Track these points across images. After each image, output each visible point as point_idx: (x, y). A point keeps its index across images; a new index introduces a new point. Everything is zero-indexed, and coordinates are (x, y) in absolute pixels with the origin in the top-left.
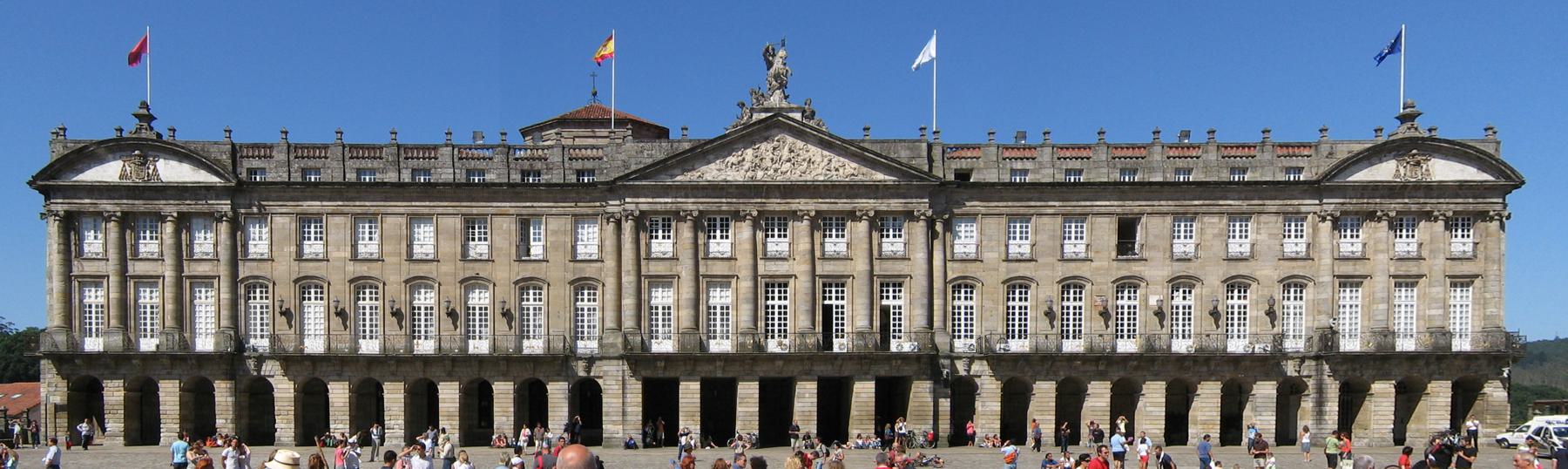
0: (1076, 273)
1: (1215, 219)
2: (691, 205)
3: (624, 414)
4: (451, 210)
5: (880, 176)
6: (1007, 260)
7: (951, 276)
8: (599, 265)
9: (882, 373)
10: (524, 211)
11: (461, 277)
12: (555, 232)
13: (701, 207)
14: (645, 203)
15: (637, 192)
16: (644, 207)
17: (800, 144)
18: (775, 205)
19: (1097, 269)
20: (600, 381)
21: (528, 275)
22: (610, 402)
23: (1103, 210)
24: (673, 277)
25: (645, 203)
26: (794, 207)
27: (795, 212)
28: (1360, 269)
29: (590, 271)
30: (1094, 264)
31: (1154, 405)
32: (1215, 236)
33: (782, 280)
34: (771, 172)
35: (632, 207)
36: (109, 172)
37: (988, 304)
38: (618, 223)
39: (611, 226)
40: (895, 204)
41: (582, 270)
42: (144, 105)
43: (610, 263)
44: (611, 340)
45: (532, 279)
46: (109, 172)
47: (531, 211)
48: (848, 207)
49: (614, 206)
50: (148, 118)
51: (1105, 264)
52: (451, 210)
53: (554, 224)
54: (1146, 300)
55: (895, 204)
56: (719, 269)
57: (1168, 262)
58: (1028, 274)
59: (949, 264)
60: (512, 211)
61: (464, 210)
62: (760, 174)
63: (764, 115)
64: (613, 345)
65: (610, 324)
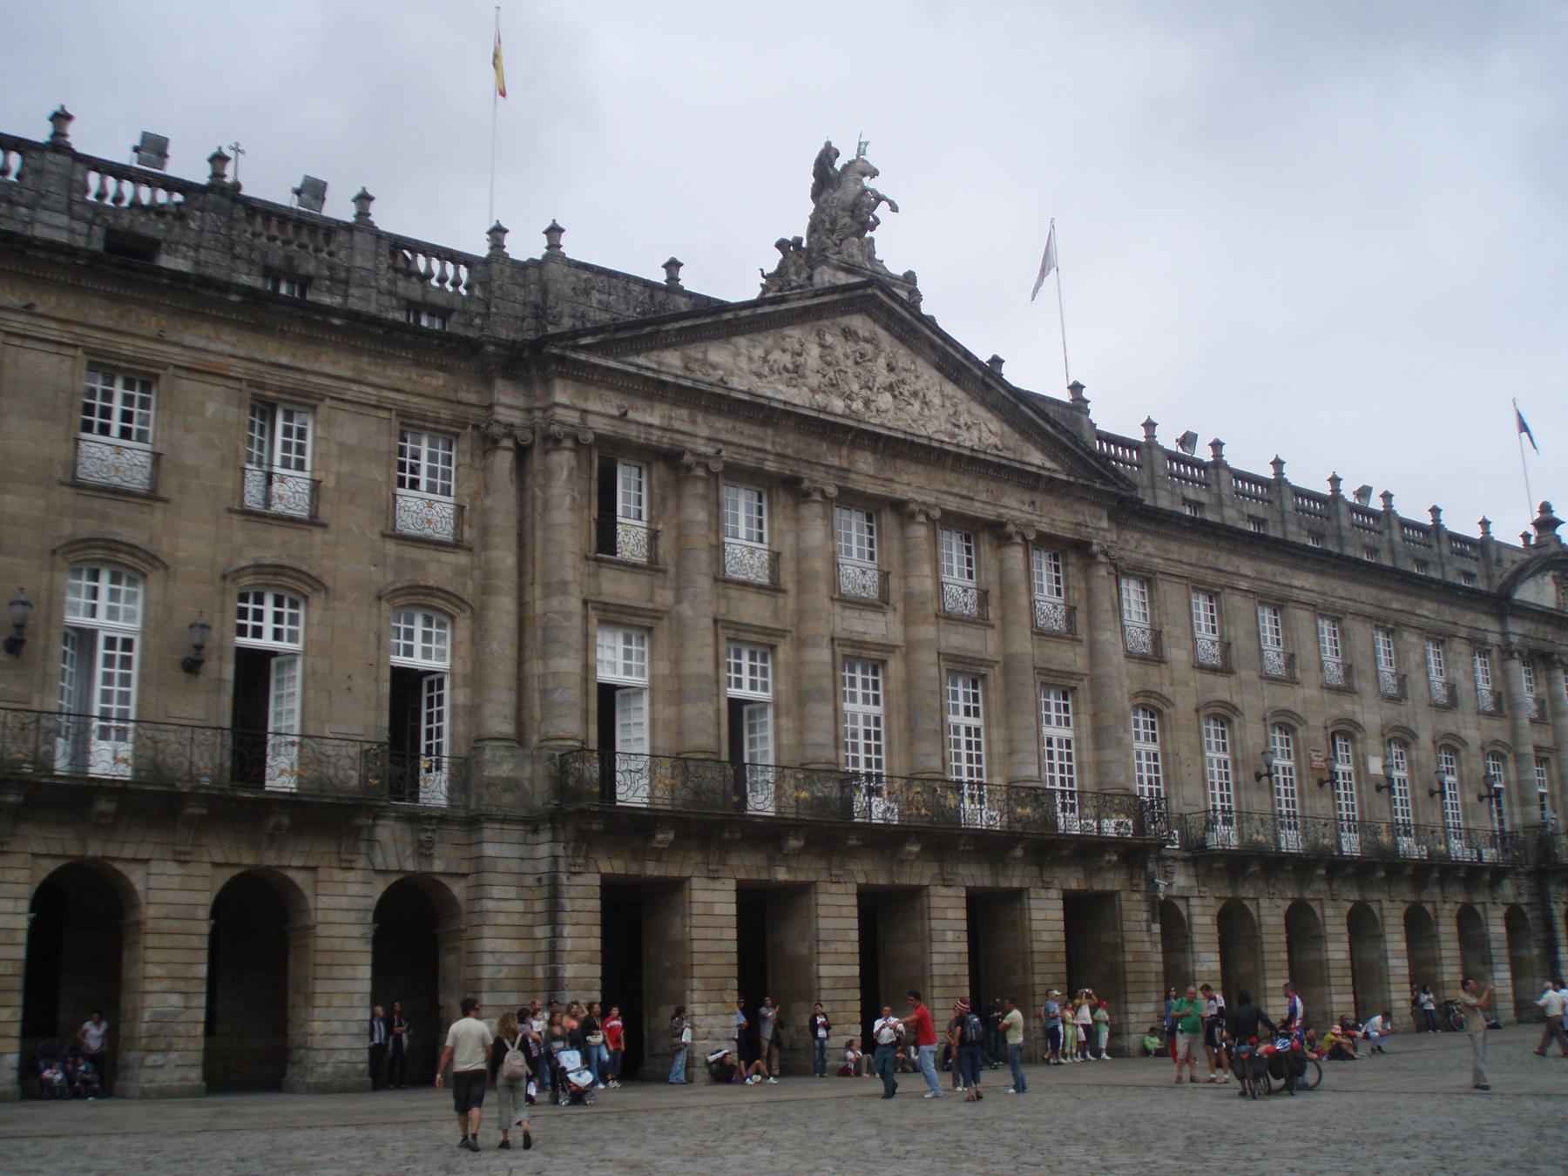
0: (1285, 705)
2: (701, 434)
3: (554, 983)
4: (53, 331)
5: (1035, 458)
6: (1201, 667)
8: (462, 559)
9: (1073, 885)
10: (273, 378)
11: (67, 529)
12: (346, 451)
14: (600, 410)
15: (586, 376)
17: (903, 357)
18: (865, 470)
20: (458, 889)
21: (269, 557)
22: (498, 946)
23: (1303, 596)
24: (657, 614)
25: (600, 410)
26: (901, 491)
27: (899, 507)
29: (440, 570)
30: (1301, 692)
33: (875, 655)
34: (858, 405)
35: (572, 417)
37: (1185, 753)
38: (522, 454)
39: (503, 461)
40: (1059, 519)
41: (418, 565)
43: (504, 558)
44: (505, 770)
45: (279, 570)
47: (291, 380)
48: (990, 513)
49: (508, 403)
52: (53, 331)
53: (351, 429)
54: (1365, 764)
55: (1059, 519)
56: (754, 610)
58: (1226, 697)
60: (238, 368)
61: (96, 339)
62: (838, 405)
63: (843, 279)
64: (511, 785)
65: (499, 722)
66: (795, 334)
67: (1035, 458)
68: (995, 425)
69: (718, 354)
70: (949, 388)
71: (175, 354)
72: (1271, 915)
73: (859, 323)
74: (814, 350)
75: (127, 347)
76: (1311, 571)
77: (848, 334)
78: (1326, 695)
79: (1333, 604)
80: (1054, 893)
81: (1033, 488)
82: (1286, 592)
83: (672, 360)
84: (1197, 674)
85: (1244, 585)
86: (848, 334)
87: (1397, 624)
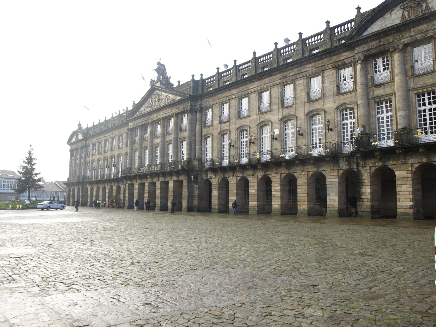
1: (302, 81)
7: (203, 134)
9: (175, 179)
13: (141, 124)
16: (132, 127)
19: (252, 120)
28: (388, 90)
30: (251, 118)
31: (276, 190)
32: (301, 90)
36: (74, 140)
42: (80, 122)
46: (74, 140)
50: (80, 125)
51: (255, 117)
57: (281, 110)
59: (203, 130)
66: (149, 100)
67: (178, 98)
68: (171, 96)
69: (141, 109)
70: (167, 94)
71: (115, 135)
72: (233, 182)
73: (155, 92)
74: (151, 101)
75: (113, 136)
76: (255, 82)
77: (155, 95)
78: (258, 116)
79: (263, 87)
80: (172, 181)
81: (176, 105)
82: (247, 92)
83: (138, 113)
84: (219, 125)
85: (233, 97)
86: (155, 95)
87: (292, 80)
